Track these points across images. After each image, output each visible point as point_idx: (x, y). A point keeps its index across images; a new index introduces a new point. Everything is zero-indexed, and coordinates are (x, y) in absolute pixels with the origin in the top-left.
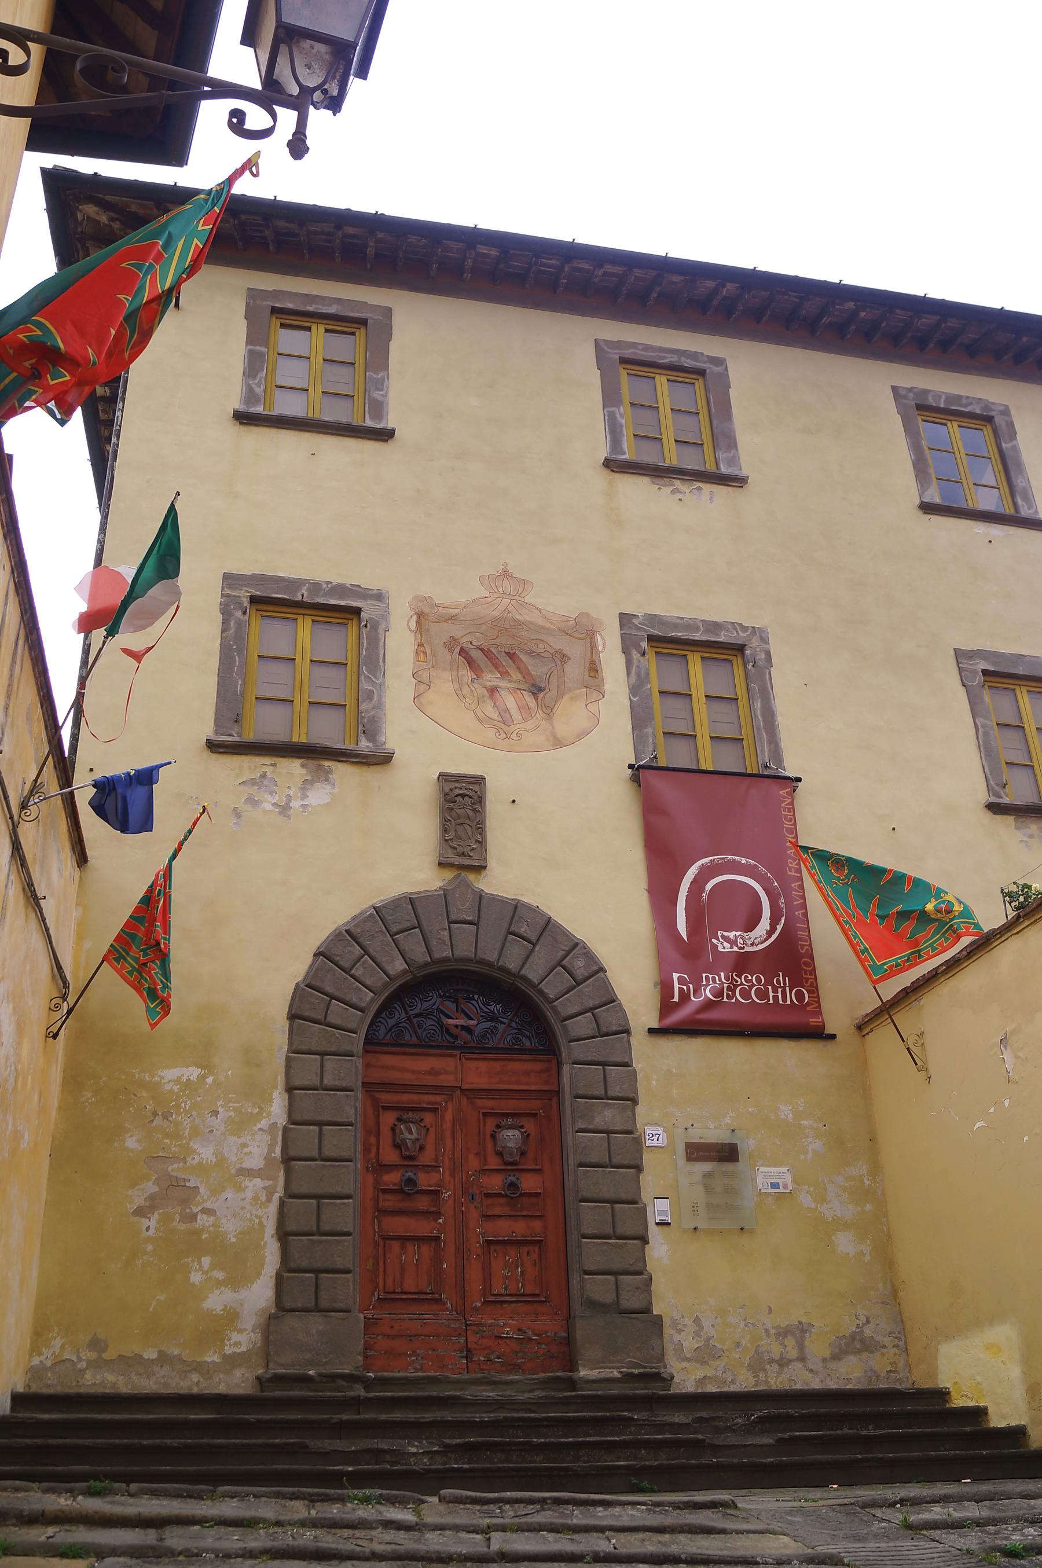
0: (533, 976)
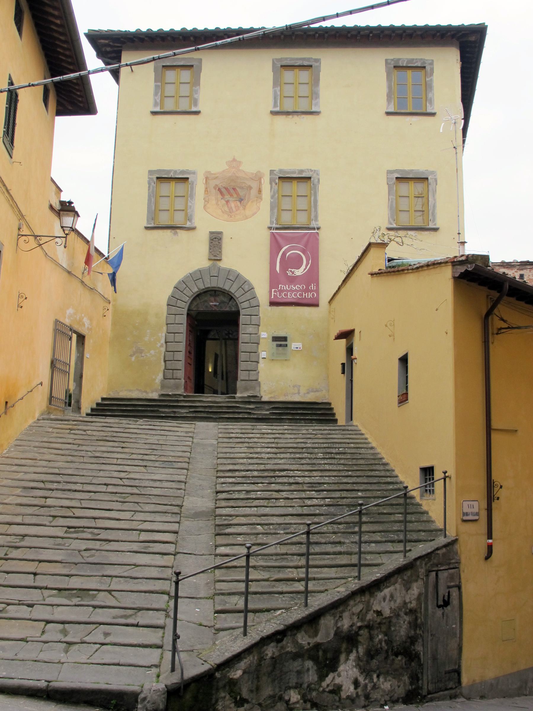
0: (233, 291)
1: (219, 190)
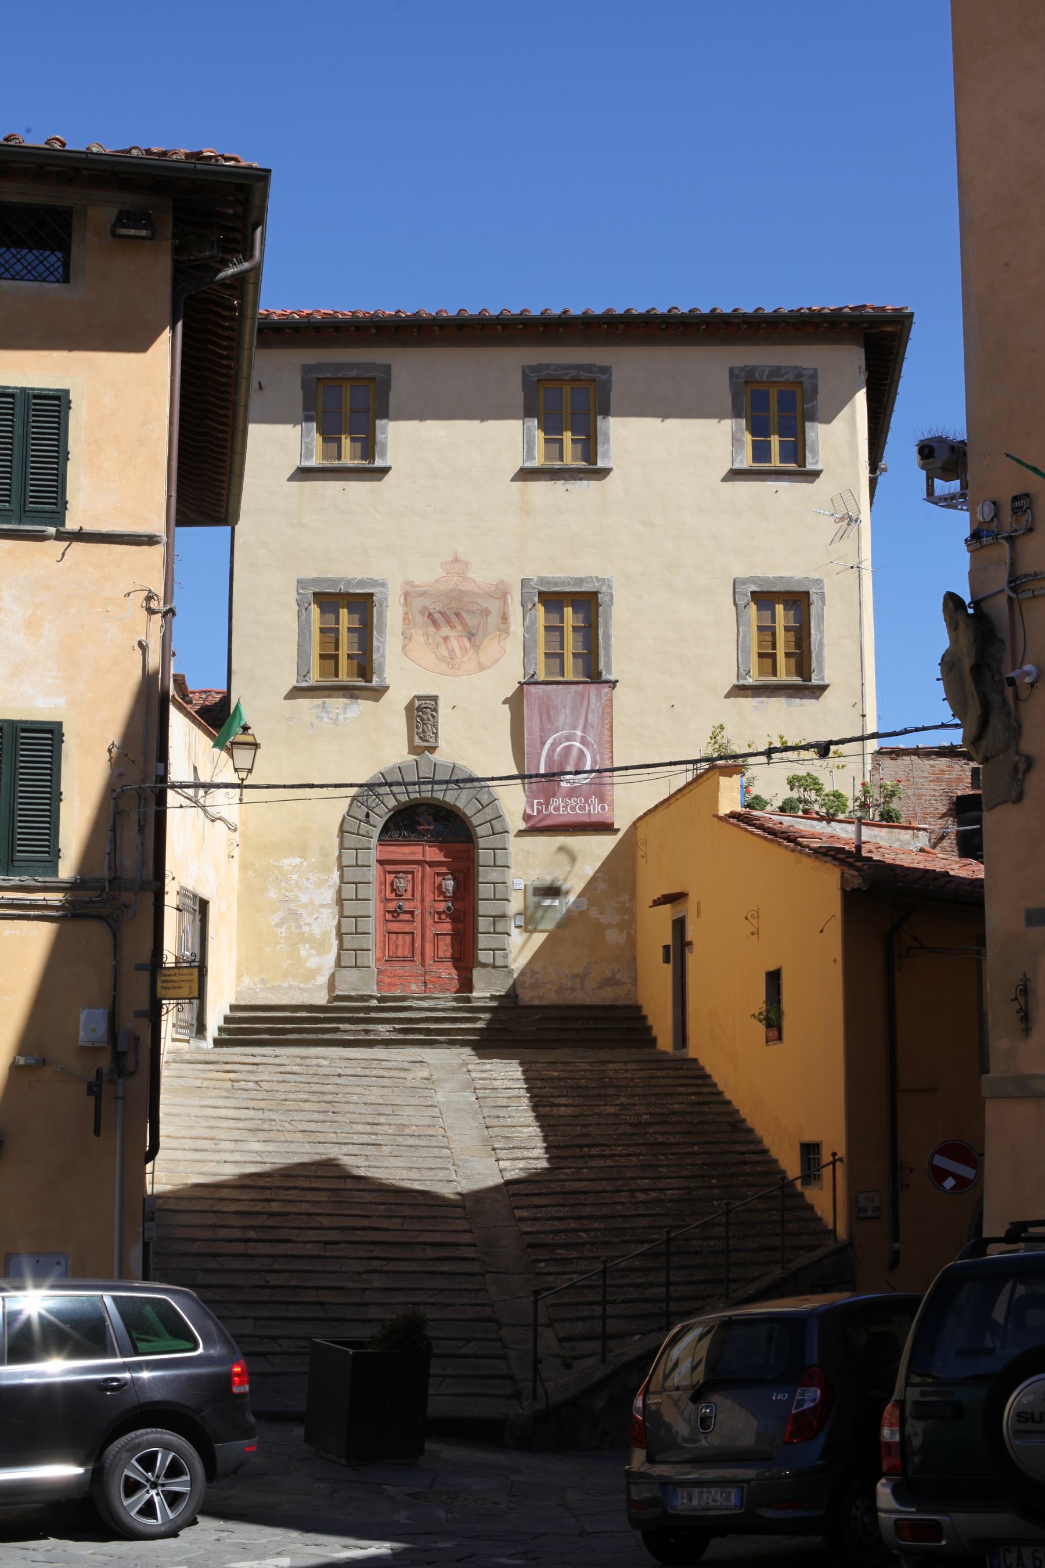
1: (430, 616)
